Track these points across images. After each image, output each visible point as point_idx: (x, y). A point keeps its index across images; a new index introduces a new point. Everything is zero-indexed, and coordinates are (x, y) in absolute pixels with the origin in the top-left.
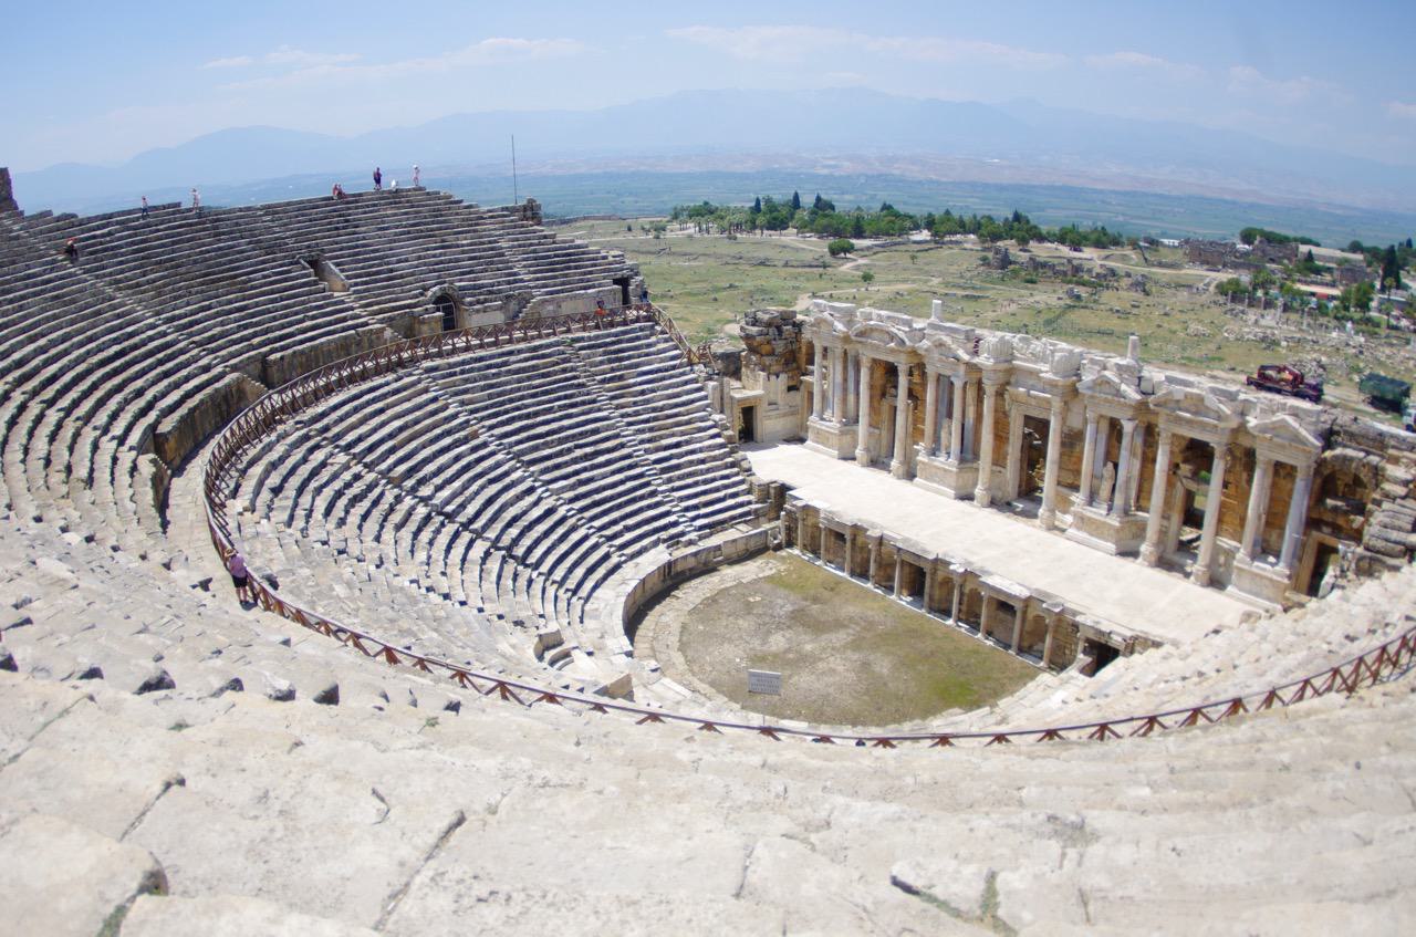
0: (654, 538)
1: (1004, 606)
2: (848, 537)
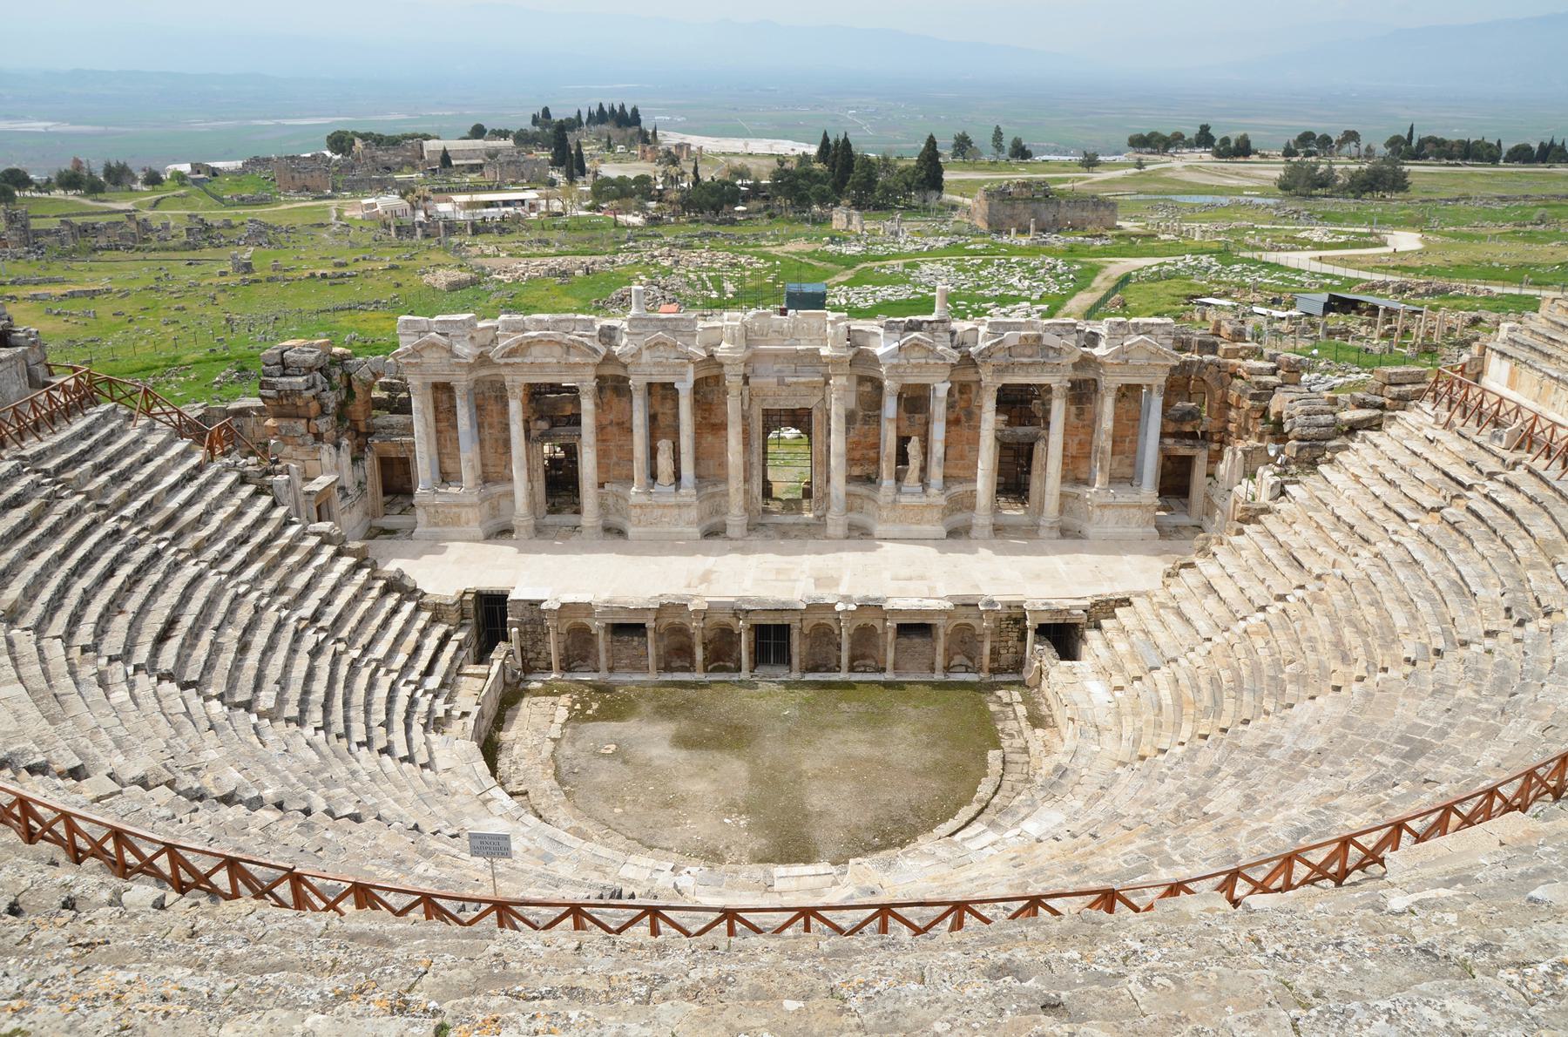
0: (417, 729)
1: (915, 629)
2: (650, 624)
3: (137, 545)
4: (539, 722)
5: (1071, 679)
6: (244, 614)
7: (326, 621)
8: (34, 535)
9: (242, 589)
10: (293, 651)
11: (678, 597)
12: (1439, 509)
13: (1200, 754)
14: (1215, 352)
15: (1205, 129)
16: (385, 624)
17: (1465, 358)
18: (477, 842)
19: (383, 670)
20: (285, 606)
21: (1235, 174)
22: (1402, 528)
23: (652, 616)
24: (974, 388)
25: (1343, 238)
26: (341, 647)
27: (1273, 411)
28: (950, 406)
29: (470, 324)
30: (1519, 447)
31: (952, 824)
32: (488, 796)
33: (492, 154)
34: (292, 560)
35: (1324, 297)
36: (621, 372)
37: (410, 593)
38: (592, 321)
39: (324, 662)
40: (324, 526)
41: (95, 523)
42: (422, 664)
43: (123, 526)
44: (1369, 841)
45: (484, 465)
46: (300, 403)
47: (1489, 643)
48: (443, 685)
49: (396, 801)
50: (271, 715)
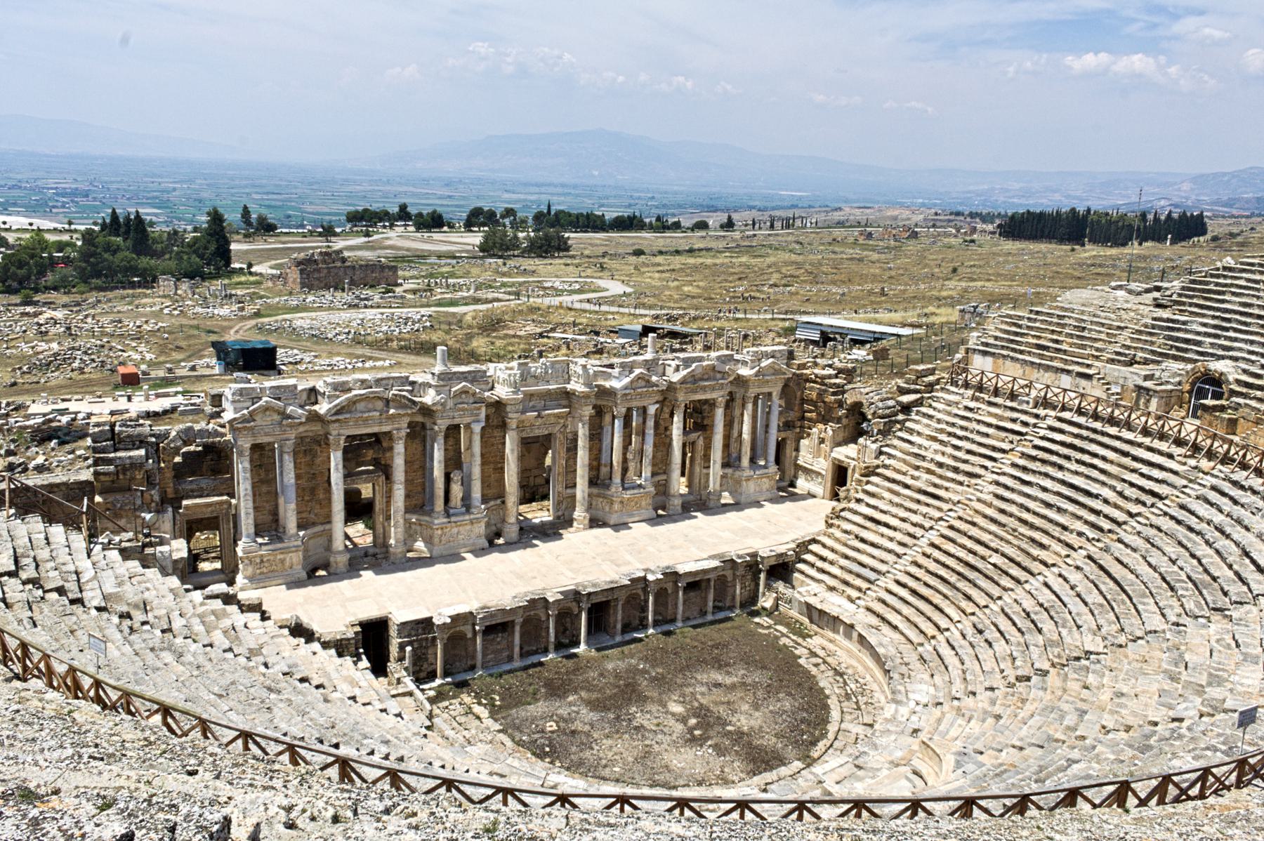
12: (1012, 450)
15: (403, 208)
21: (440, 241)
25: (577, 287)
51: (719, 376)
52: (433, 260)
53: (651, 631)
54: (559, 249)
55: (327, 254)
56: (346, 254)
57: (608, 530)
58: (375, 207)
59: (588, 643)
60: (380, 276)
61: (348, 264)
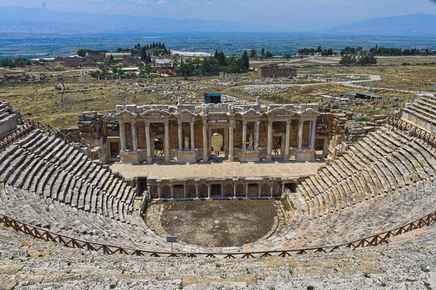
0: (125, 214)
1: (253, 185)
2: (185, 185)
3: (49, 167)
4: (156, 212)
5: (295, 197)
6: (78, 185)
7: (100, 186)
8: (23, 165)
9: (77, 178)
10: (92, 194)
11: (192, 177)
12: (391, 152)
13: (332, 217)
14: (329, 112)
15: (319, 48)
16: (115, 187)
17: (396, 112)
18: (168, 239)
19: (115, 199)
20: (89, 182)
22: (382, 157)
23: (185, 183)
24: (266, 123)
25: (359, 77)
26: (104, 192)
27: (345, 127)
28: (260, 127)
29: (136, 107)
30: (412, 136)
31: (266, 236)
32: (146, 231)
33: (125, 57)
34: (90, 170)
35: (355, 94)
36: (175, 120)
37: (120, 178)
38: (168, 107)
39: (100, 196)
40: (97, 161)
41: (38, 162)
42: (125, 197)
43: (45, 161)
44: (382, 236)
45: (138, 144)
46: (89, 128)
47: (407, 187)
48: (131, 202)
49: (124, 233)
50: (89, 211)
51: (286, 113)
52: (321, 67)
53: (234, 197)
54: (372, 63)
55: (271, 65)
56: (279, 65)
57: (239, 163)
58: (309, 48)
59: (211, 197)
60: (290, 73)
61: (278, 68)
